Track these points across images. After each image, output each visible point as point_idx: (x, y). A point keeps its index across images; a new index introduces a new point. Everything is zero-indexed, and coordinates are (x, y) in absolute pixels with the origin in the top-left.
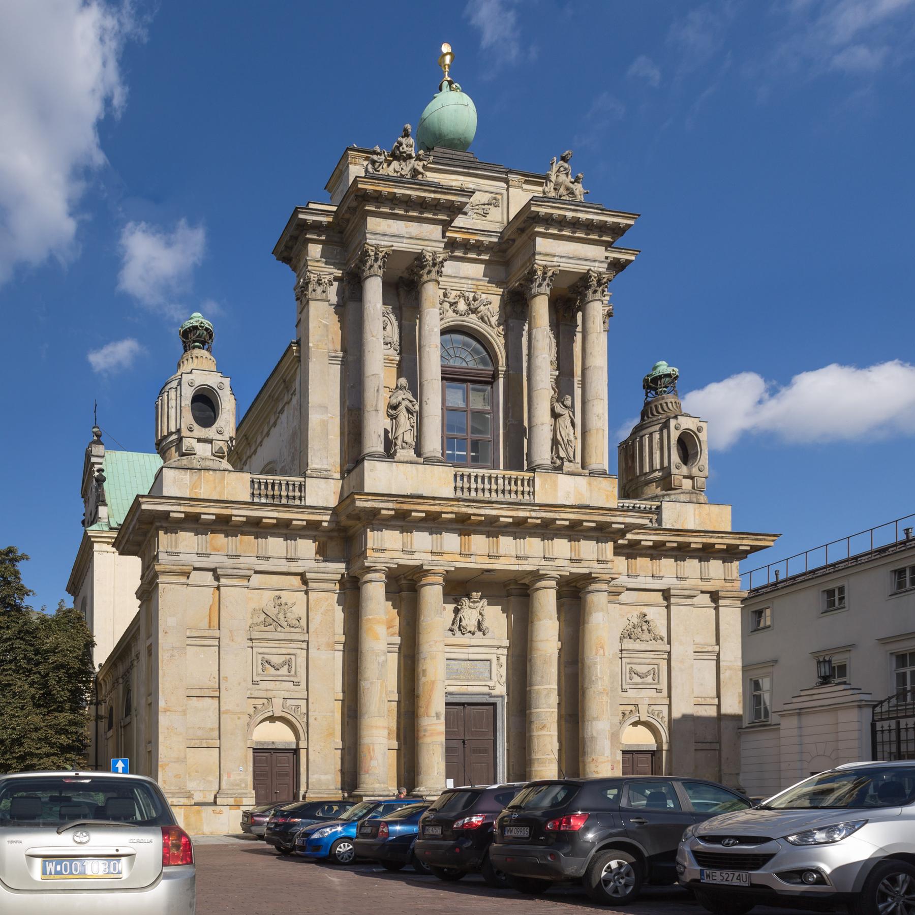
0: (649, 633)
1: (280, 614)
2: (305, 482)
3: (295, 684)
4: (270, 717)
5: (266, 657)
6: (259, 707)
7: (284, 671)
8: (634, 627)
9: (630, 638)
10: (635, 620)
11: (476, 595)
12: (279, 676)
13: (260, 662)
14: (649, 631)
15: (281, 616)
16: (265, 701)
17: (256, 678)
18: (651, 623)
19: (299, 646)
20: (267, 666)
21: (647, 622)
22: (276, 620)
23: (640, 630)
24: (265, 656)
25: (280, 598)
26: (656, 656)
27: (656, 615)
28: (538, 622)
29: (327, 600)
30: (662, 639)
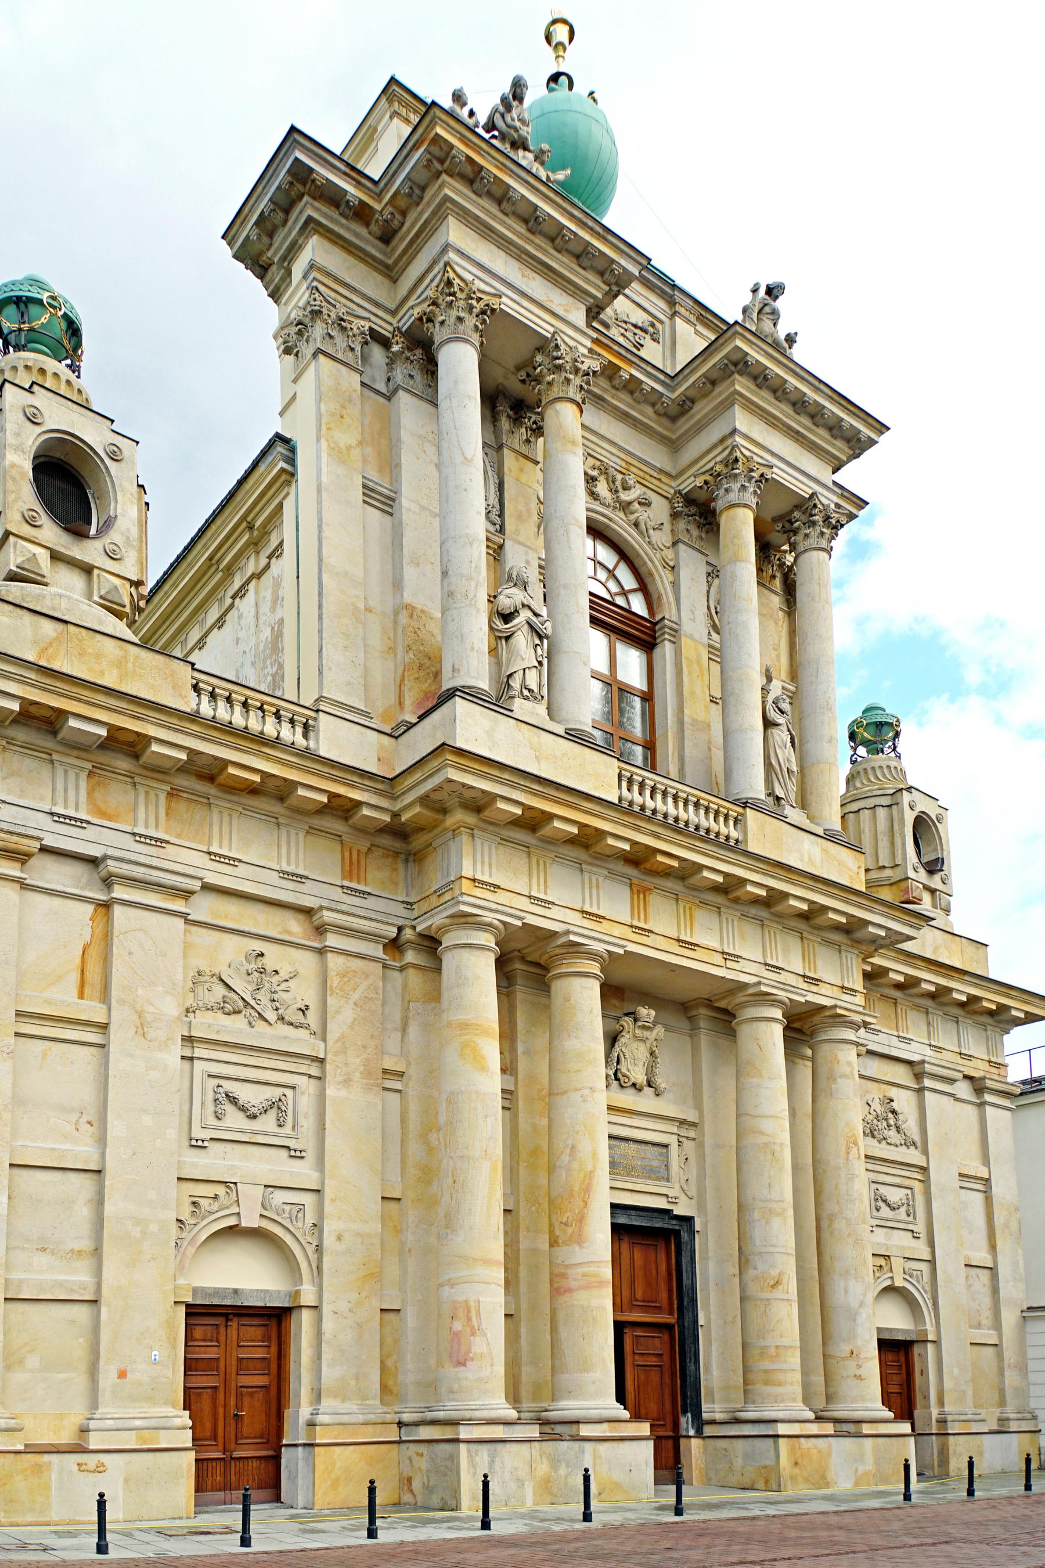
0: (899, 1132)
1: (262, 991)
2: (315, 719)
3: (293, 1153)
4: (231, 1228)
5: (228, 1086)
6: (204, 1203)
7: (267, 1123)
8: (877, 1117)
9: (873, 1136)
10: (876, 1106)
11: (646, 1013)
12: (257, 1133)
13: (210, 1096)
14: (898, 1128)
15: (264, 996)
16: (220, 1190)
17: (198, 1133)
18: (900, 1117)
19: (303, 1069)
20: (229, 1108)
21: (894, 1112)
22: (252, 1003)
23: (885, 1124)
24: (221, 1082)
25: (262, 955)
26: (907, 1174)
27: (904, 1101)
28: (755, 1081)
29: (367, 976)
30: (914, 1144)
